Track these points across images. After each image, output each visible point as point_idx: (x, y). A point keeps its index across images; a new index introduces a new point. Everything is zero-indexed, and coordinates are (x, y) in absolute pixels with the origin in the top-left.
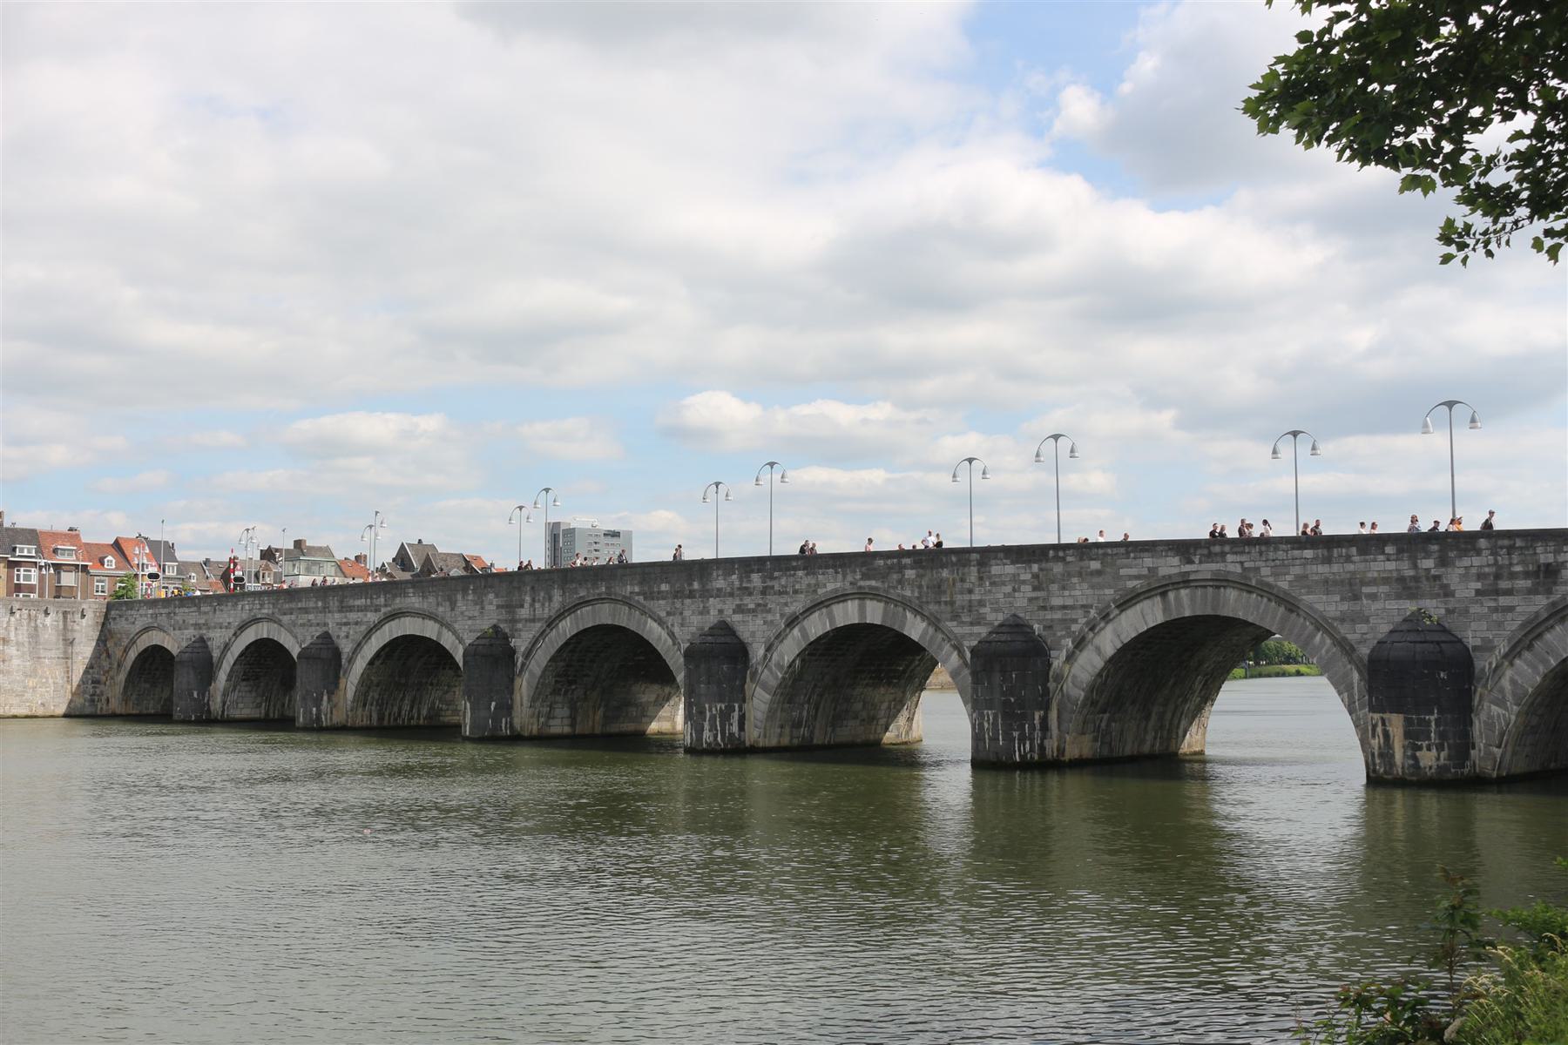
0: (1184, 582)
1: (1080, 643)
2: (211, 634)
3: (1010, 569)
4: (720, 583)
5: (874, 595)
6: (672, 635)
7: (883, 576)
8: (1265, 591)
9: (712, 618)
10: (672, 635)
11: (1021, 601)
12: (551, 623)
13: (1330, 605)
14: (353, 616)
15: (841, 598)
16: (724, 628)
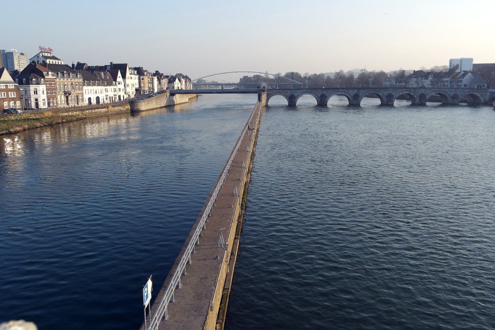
0: (438, 91)
1: (428, 95)
2: (295, 94)
3: (422, 89)
4: (390, 90)
5: (408, 91)
6: (383, 94)
7: (409, 89)
8: (444, 92)
9: (389, 93)
10: (383, 94)
11: (423, 92)
12: (365, 93)
13: (449, 93)
14: (329, 92)
15: (403, 91)
16: (390, 94)
